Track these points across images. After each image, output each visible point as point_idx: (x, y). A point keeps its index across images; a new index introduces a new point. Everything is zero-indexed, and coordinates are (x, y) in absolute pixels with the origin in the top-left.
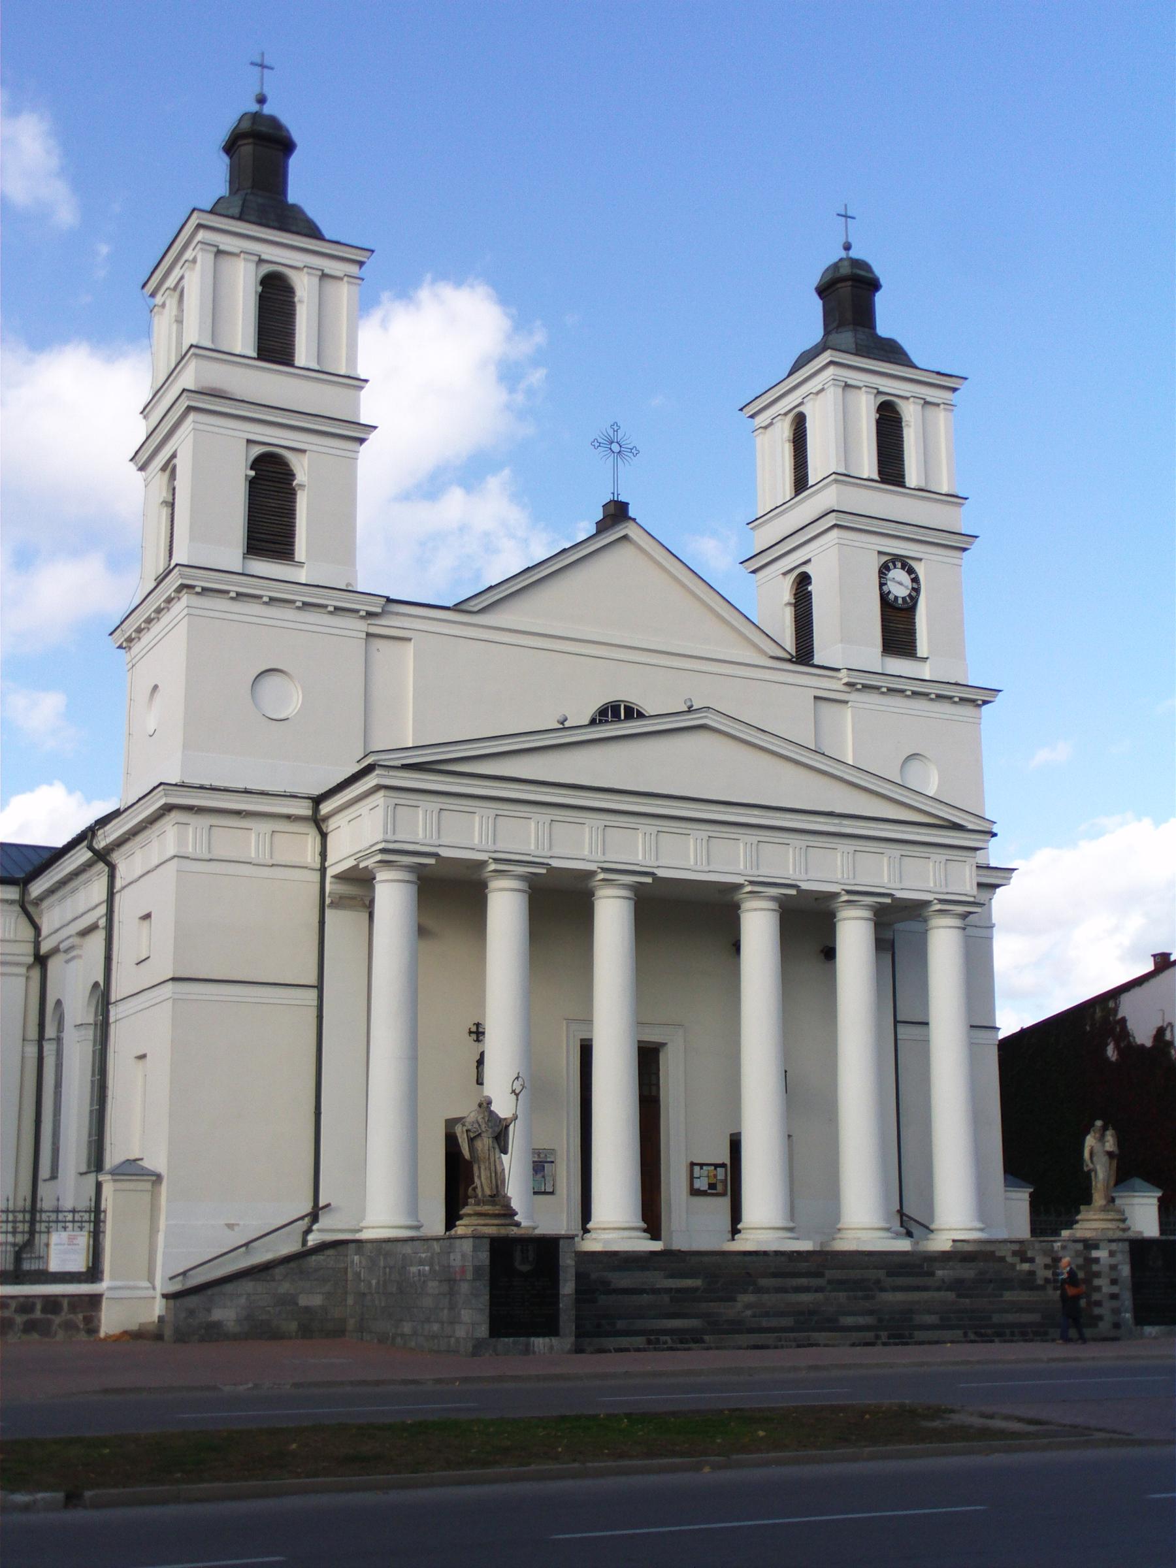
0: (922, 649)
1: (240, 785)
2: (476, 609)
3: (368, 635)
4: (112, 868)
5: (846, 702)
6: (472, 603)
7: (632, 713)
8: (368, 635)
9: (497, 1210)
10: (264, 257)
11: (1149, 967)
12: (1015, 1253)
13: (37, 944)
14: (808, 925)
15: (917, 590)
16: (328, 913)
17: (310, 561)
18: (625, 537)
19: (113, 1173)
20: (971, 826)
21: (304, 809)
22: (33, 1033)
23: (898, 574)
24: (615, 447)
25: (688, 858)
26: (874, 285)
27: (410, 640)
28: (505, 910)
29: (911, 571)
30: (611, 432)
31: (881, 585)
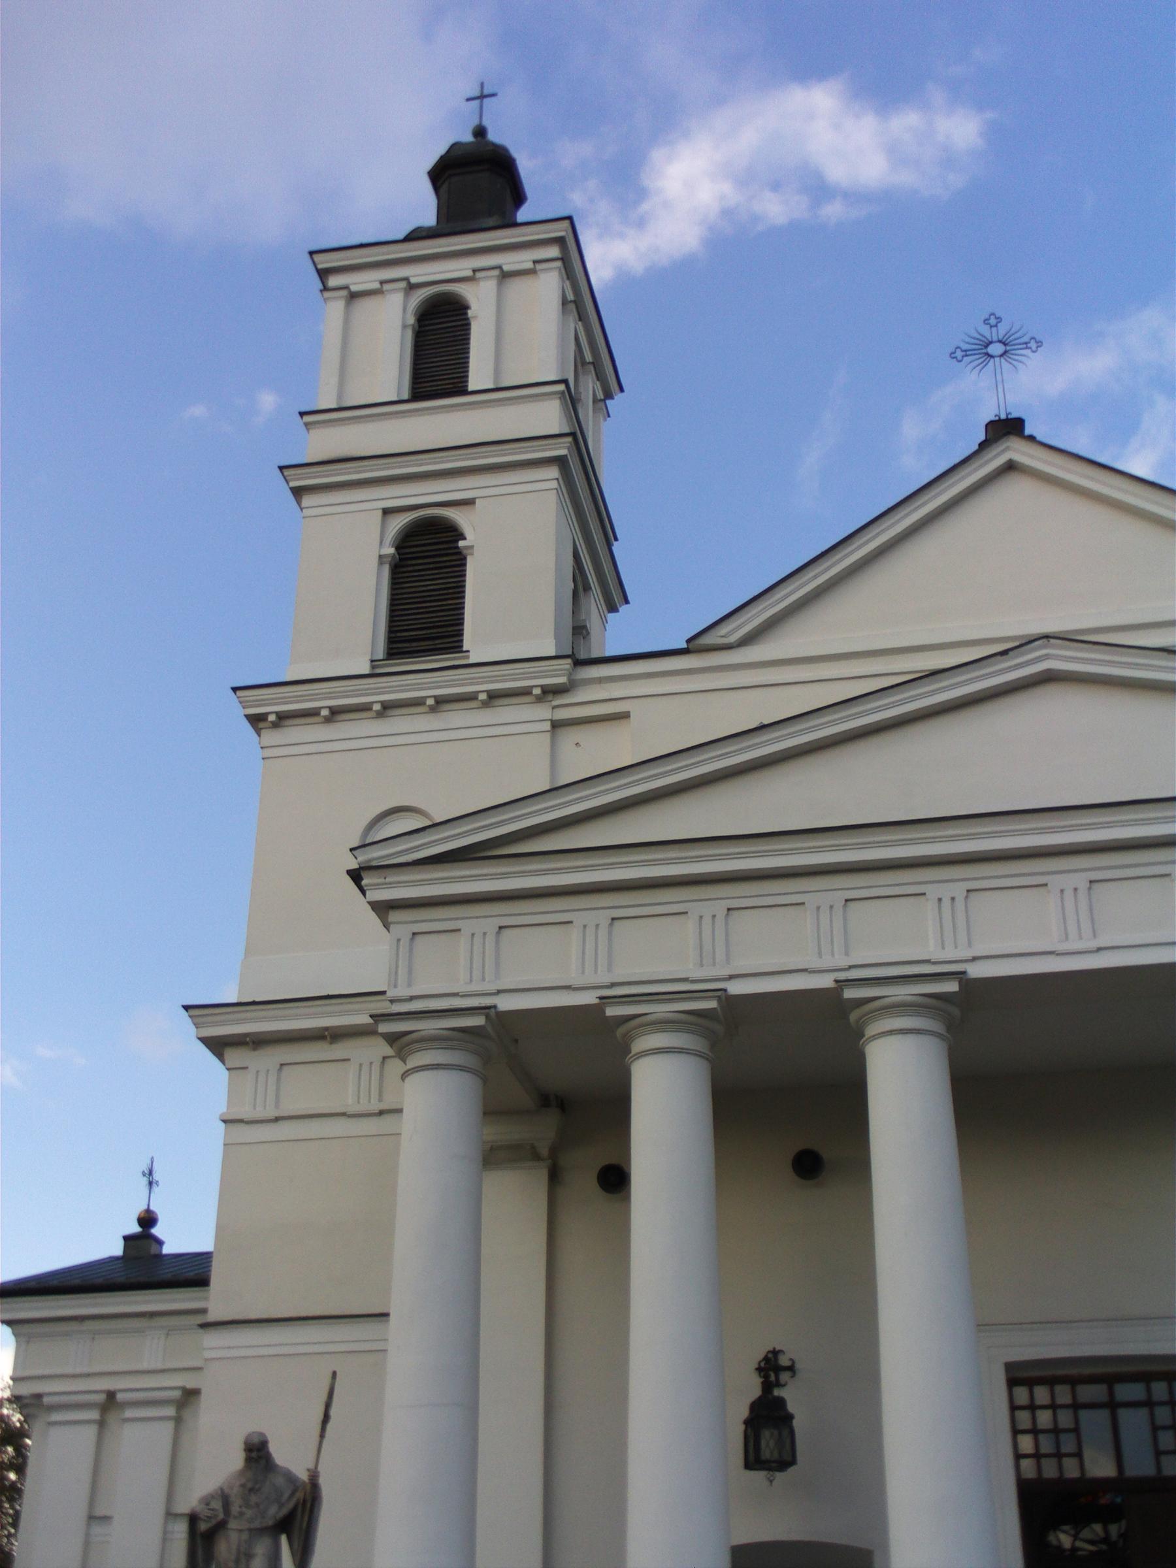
2: (732, 639)
3: (556, 725)
6: (723, 630)
8: (556, 725)
10: (413, 280)
18: (1011, 467)
27: (625, 716)
28: (665, 1104)
30: (985, 330)
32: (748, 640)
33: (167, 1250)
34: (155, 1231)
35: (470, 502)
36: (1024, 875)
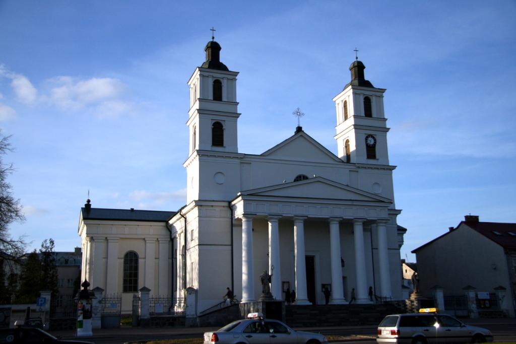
0: (377, 157)
1: (212, 200)
3: (241, 163)
4: (185, 218)
5: (357, 171)
7: (305, 178)
8: (241, 163)
9: (268, 296)
11: (448, 230)
12: (396, 304)
13: (171, 236)
14: (347, 226)
15: (375, 142)
16: (234, 228)
17: (227, 148)
18: (301, 136)
19: (141, 290)
20: (385, 201)
21: (226, 204)
22: (171, 257)
23: (370, 139)
24: (298, 114)
25: (315, 212)
26: (364, 67)
27: (250, 163)
29: (373, 138)
31: (366, 142)
32: (267, 156)
33: (92, 207)
34: (90, 203)
35: (224, 121)
36: (191, 122)
